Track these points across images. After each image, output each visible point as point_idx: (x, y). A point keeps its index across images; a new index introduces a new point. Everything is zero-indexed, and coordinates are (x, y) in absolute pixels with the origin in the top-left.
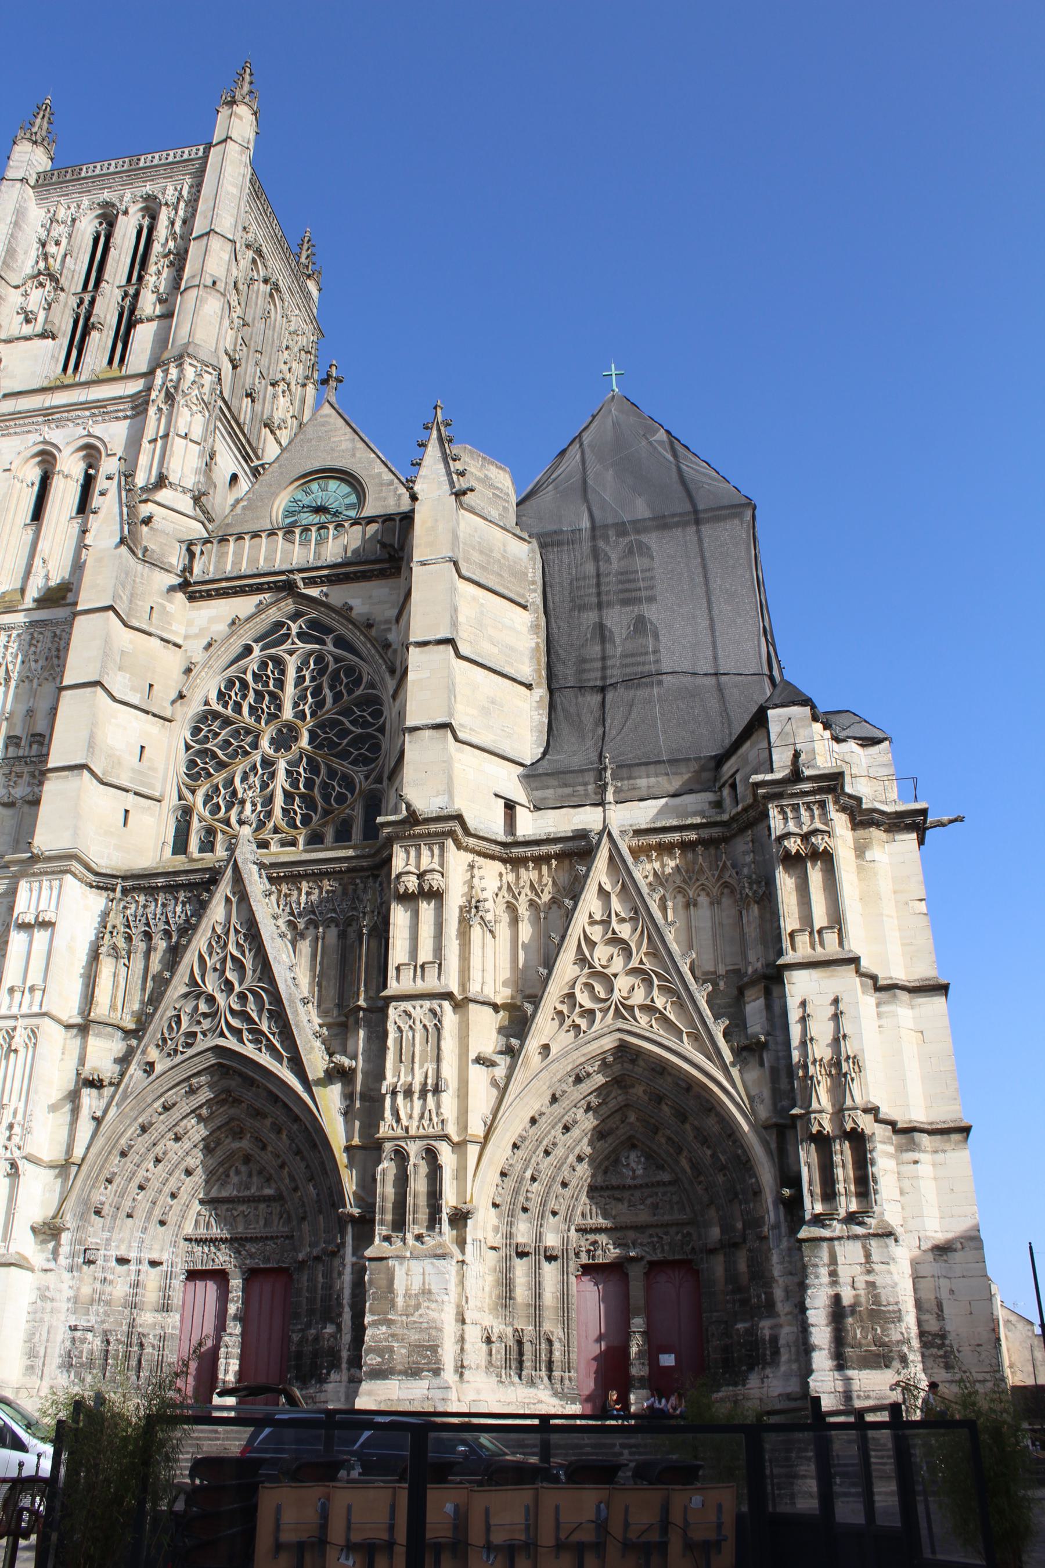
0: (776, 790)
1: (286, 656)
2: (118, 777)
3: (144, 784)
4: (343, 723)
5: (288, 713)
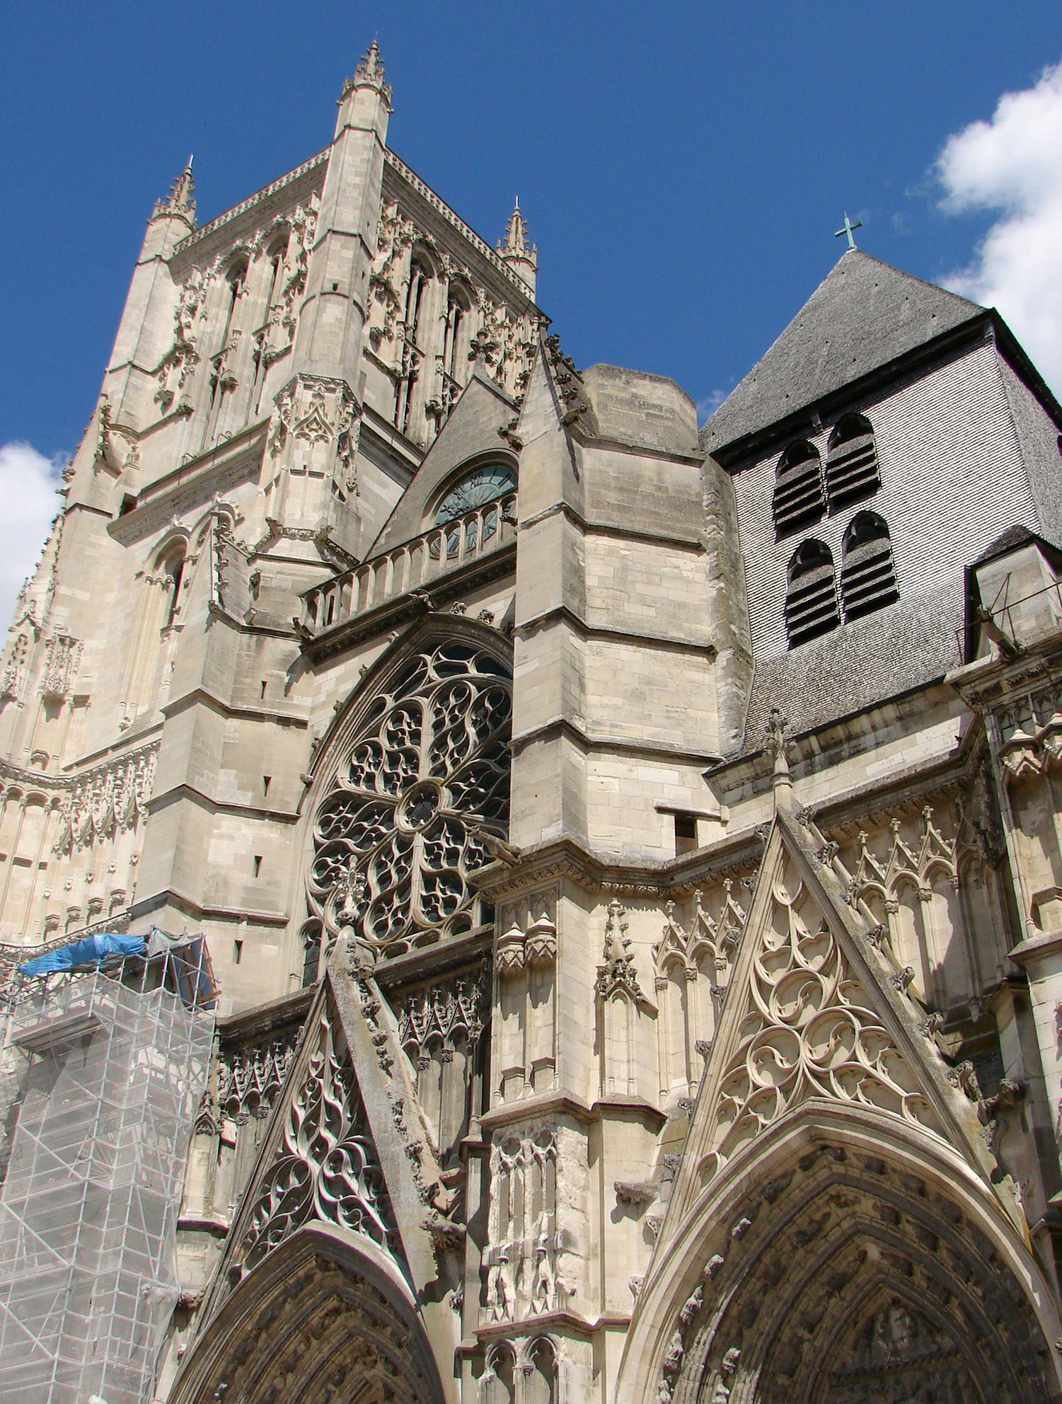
0: (987, 685)
1: (424, 701)
2: (225, 901)
3: (261, 905)
4: (487, 767)
5: (424, 773)
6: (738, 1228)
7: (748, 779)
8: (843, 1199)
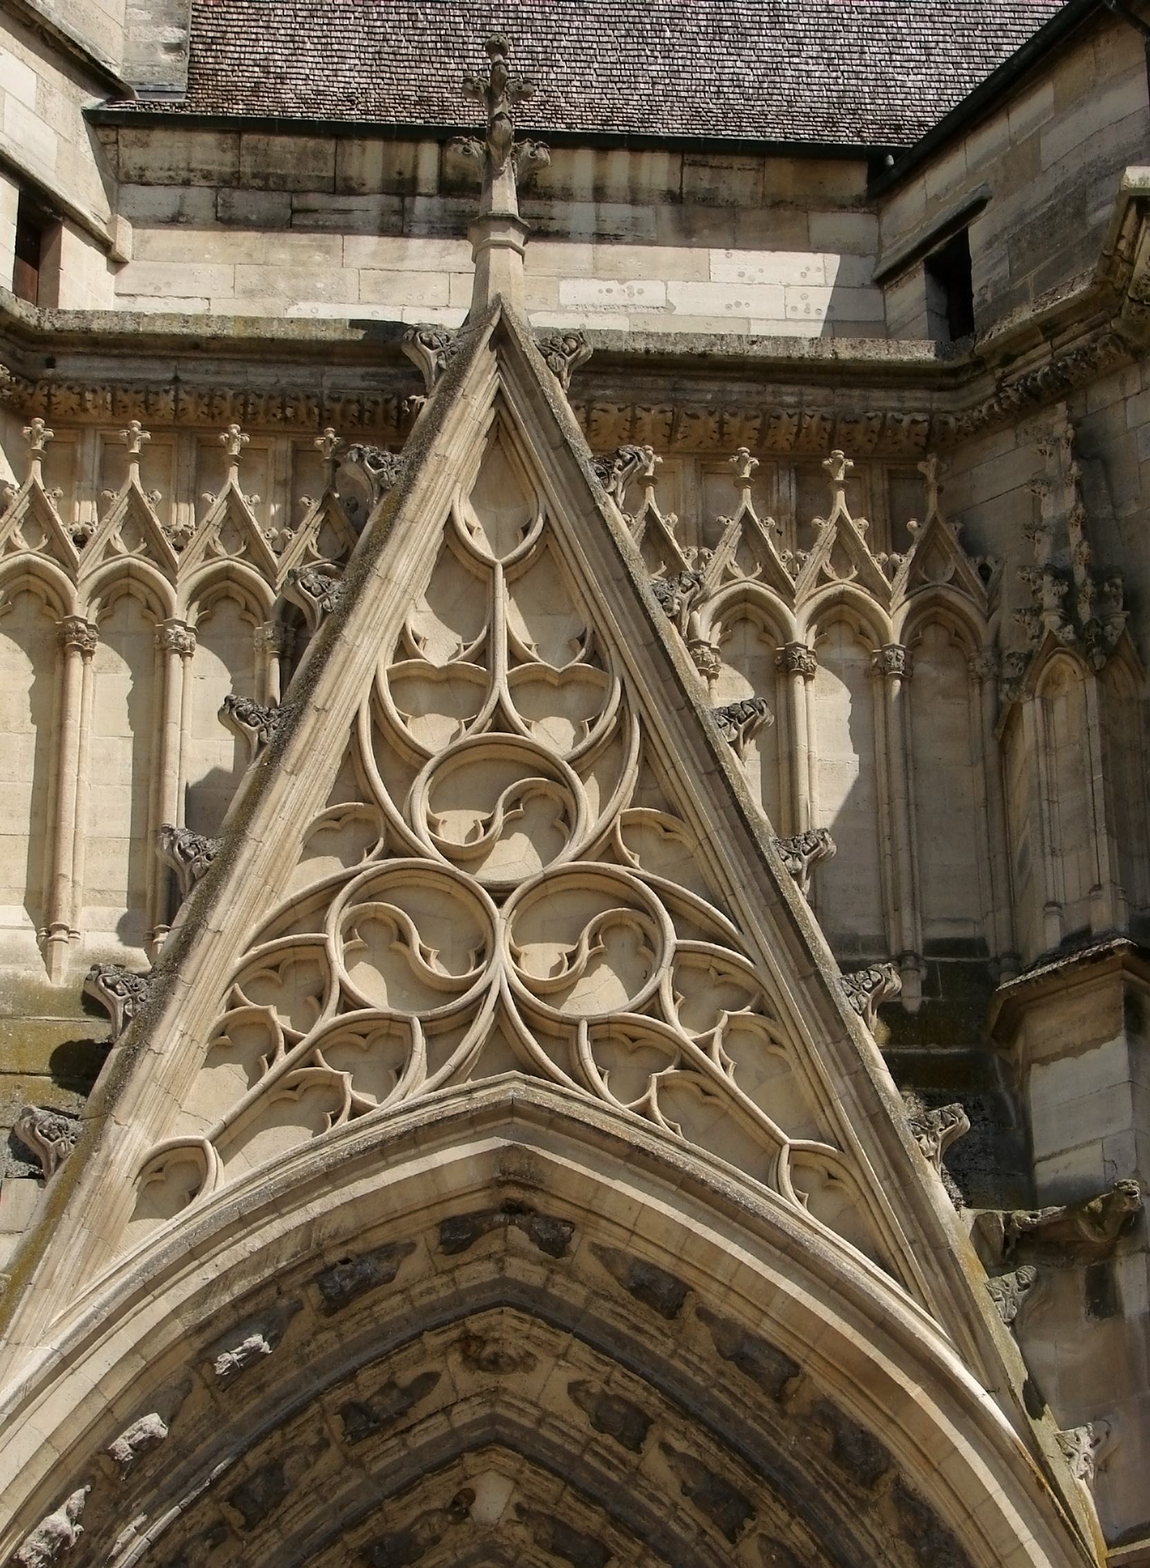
6: (234, 1356)
7: (207, 176)
8: (489, 1350)
